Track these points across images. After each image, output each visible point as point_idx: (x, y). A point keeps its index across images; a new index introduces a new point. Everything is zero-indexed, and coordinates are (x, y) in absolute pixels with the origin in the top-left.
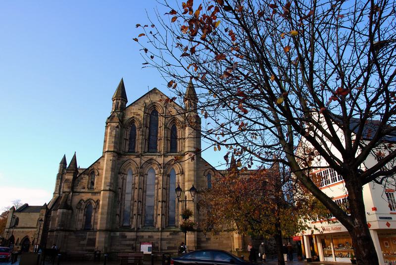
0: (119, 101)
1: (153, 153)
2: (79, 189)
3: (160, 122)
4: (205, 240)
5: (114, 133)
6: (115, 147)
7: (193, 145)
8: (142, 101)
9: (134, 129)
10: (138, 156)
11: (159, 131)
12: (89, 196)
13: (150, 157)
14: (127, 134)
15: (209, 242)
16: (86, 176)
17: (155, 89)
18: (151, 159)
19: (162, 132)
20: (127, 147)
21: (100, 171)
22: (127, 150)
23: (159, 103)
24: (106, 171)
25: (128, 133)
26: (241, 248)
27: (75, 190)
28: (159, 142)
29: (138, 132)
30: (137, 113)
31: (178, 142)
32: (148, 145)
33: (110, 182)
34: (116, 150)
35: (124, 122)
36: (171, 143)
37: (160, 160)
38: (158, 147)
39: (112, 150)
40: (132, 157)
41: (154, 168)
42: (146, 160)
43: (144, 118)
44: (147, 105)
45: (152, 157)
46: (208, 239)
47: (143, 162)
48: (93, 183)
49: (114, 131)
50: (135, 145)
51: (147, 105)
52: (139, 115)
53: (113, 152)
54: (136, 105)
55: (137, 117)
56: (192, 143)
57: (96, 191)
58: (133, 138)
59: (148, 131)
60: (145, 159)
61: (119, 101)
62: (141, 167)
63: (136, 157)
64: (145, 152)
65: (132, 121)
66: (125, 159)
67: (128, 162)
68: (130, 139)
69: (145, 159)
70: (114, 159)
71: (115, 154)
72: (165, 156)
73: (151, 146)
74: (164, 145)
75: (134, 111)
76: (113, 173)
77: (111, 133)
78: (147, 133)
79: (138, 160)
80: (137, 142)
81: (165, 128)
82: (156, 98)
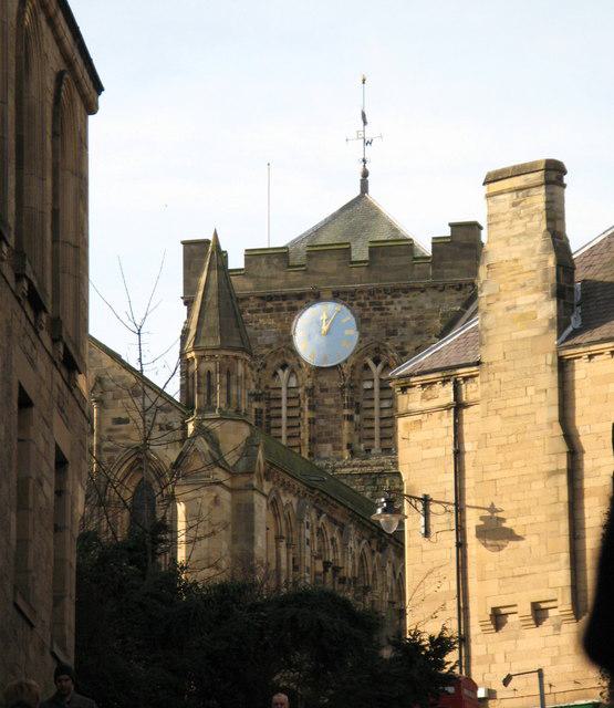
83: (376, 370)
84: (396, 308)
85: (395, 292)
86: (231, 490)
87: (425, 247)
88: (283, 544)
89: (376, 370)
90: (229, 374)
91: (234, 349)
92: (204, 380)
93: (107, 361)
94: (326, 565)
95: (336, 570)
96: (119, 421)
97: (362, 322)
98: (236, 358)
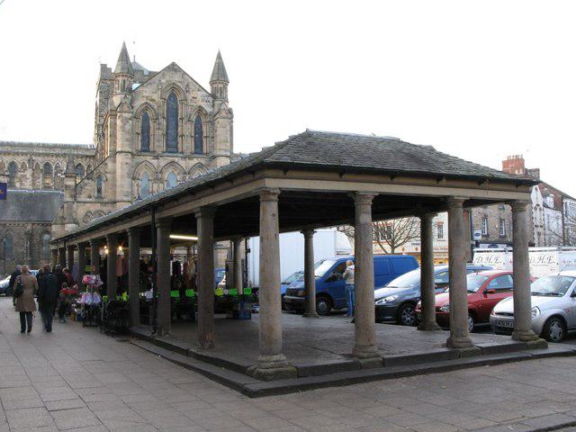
1: (174, 152)
2: (83, 198)
3: (179, 111)
5: (128, 127)
9: (146, 119)
10: (157, 158)
11: (180, 124)
12: (98, 207)
16: (90, 181)
17: (173, 64)
18: (172, 163)
19: (187, 129)
20: (140, 144)
21: (108, 176)
22: (140, 147)
24: (122, 177)
25: (140, 124)
27: (79, 200)
28: (180, 139)
31: (204, 140)
34: (130, 150)
38: (179, 146)
40: (149, 158)
41: (176, 172)
42: (166, 162)
48: (99, 191)
50: (149, 142)
51: (164, 87)
52: (153, 100)
54: (149, 86)
57: (106, 200)
58: (145, 133)
59: (165, 123)
61: (126, 79)
62: (161, 172)
64: (163, 152)
65: (147, 107)
67: (144, 164)
69: (163, 162)
71: (130, 155)
73: (172, 147)
77: (123, 127)
78: (165, 126)
79: (154, 162)
80: (152, 138)
82: (176, 78)
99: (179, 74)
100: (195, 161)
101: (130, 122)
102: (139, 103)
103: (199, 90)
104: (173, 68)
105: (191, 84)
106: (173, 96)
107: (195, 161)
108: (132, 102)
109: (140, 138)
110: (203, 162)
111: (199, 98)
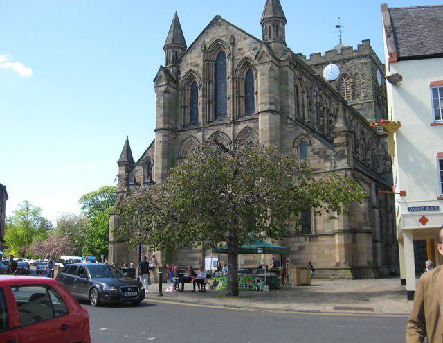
0: (171, 50)
4: (297, 249)
6: (164, 122)
7: (267, 100)
8: (200, 43)
10: (199, 130)
13: (215, 129)
14: (185, 98)
15: (302, 251)
17: (217, 18)
23: (223, 39)
25: (188, 96)
26: (343, 261)
29: (200, 93)
30: (194, 62)
32: (215, 110)
33: (162, 174)
34: (167, 126)
35: (180, 82)
36: (246, 100)
37: (228, 131)
39: (161, 126)
40: (193, 133)
43: (204, 68)
44: (208, 46)
45: (218, 127)
46: (301, 248)
47: (207, 137)
49: (162, 98)
51: (208, 46)
52: (197, 65)
53: (163, 129)
55: (195, 69)
56: (266, 97)
59: (212, 87)
60: (209, 133)
61: (171, 50)
63: (198, 132)
66: (185, 137)
68: (190, 105)
70: (166, 139)
71: (166, 132)
72: (235, 123)
74: (233, 106)
75: (192, 61)
76: (166, 160)
78: (212, 92)
79: (199, 135)
81: (233, 78)
82: (219, 33)
83: (345, 80)
84: (349, 64)
85: (349, 59)
86: (278, 66)
87: (355, 48)
88: (305, 95)
89: (345, 80)
90: (277, 27)
91: (278, 17)
92: (268, 30)
93: (235, 30)
94: (324, 108)
95: (328, 111)
96: (240, 49)
97: (340, 68)
98: (280, 21)
99: (224, 27)
100: (241, 127)
101: (167, 95)
102: (183, 73)
103: (245, 39)
104: (217, 21)
105: (236, 33)
106: (221, 54)
107: (241, 127)
108: (178, 72)
109: (188, 111)
110: (251, 125)
111: (246, 49)
